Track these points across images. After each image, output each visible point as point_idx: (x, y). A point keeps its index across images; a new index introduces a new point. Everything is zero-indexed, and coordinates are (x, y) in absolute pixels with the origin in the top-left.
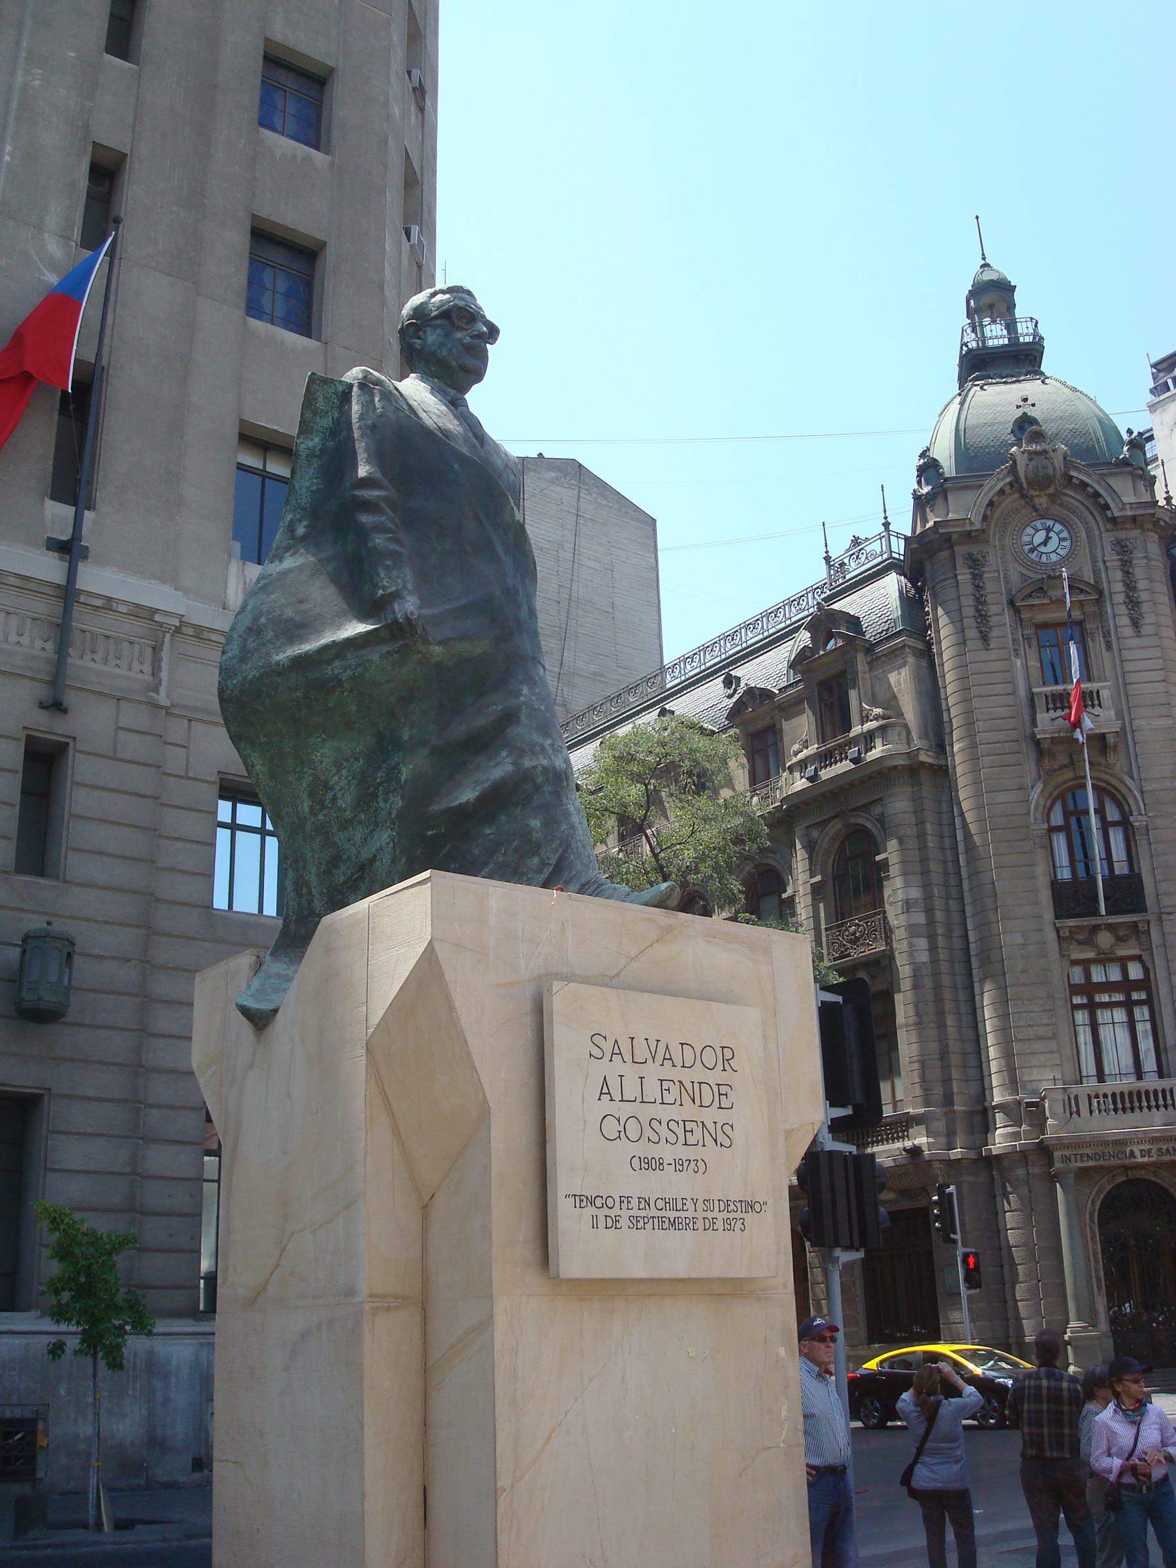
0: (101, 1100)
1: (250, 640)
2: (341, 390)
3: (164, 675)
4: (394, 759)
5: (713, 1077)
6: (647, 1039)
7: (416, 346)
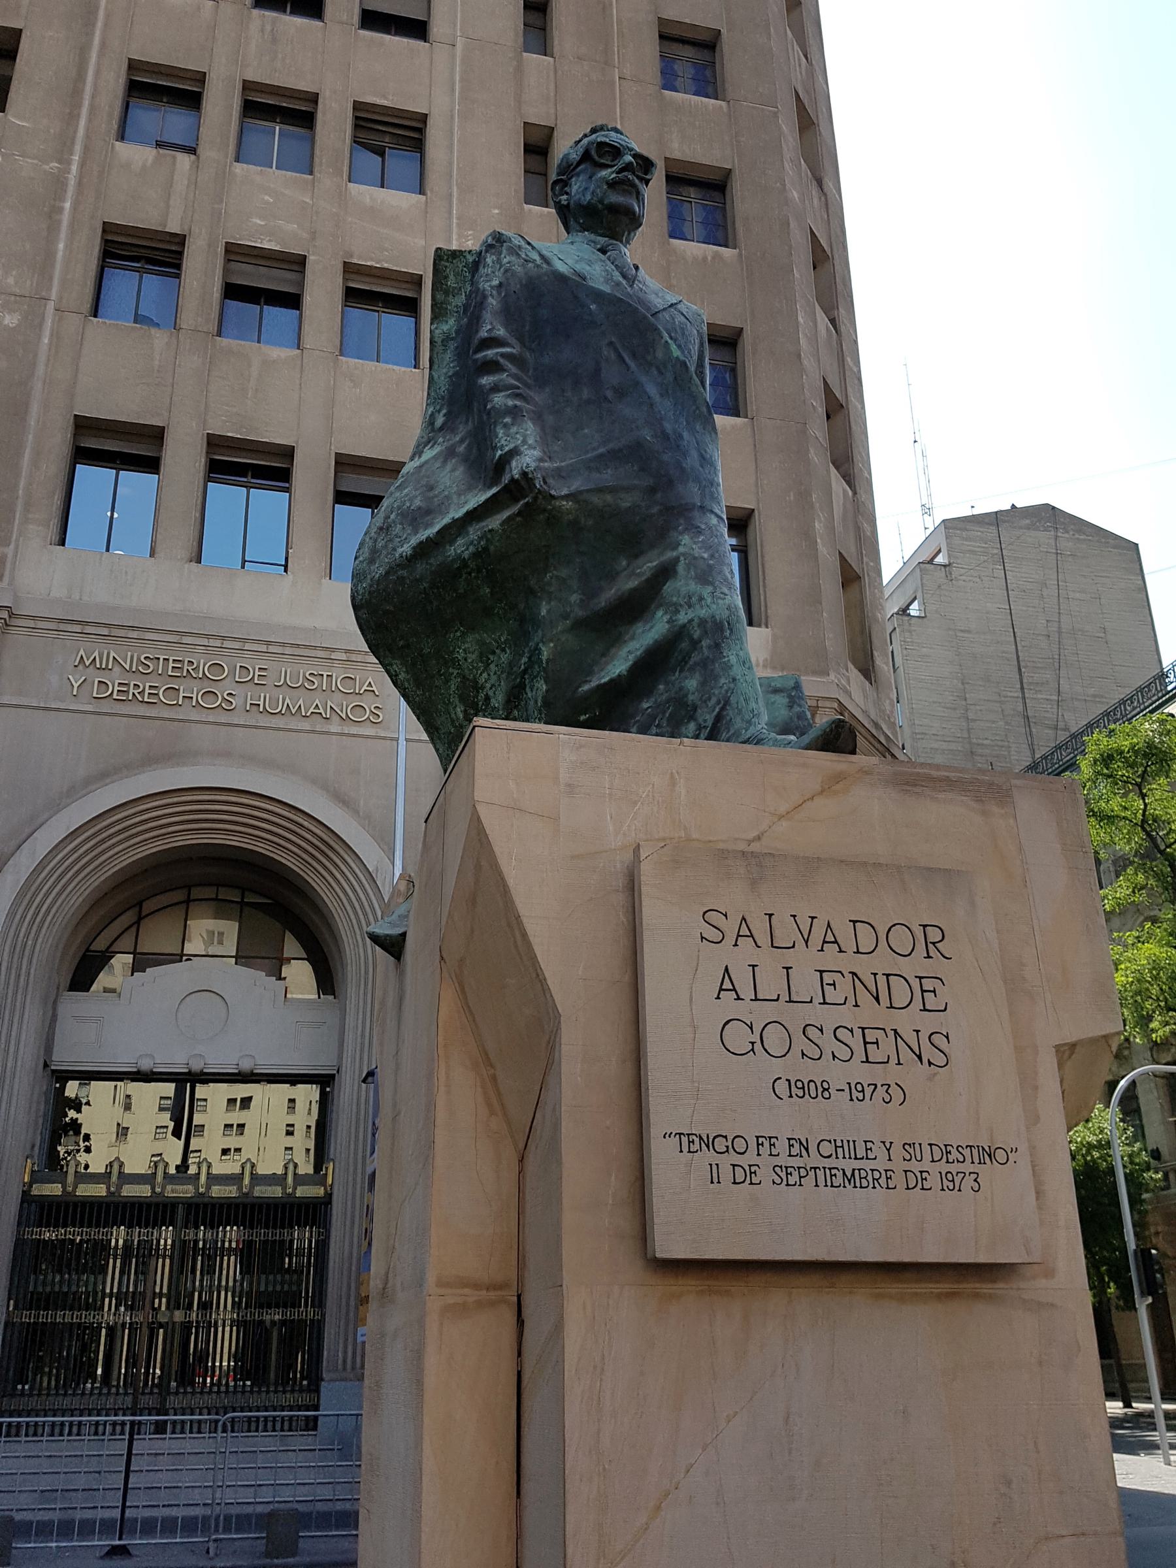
6: (794, 916)
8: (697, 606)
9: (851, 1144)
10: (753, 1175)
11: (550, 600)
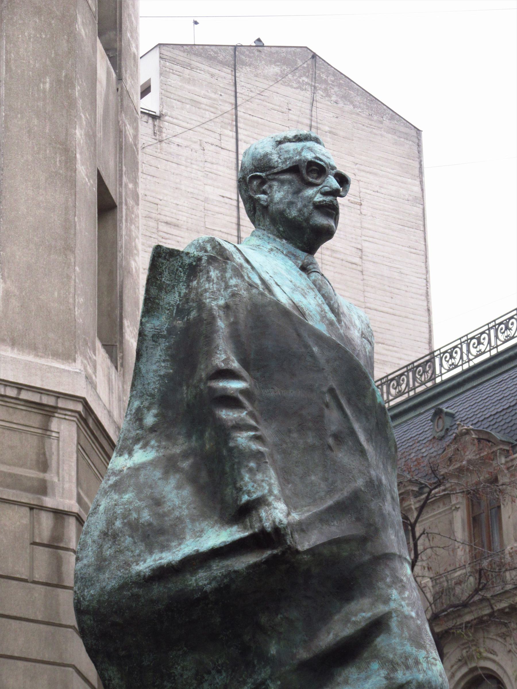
1: (105, 547)
2: (187, 262)
4: (260, 674)
7: (262, 202)
8: (415, 670)
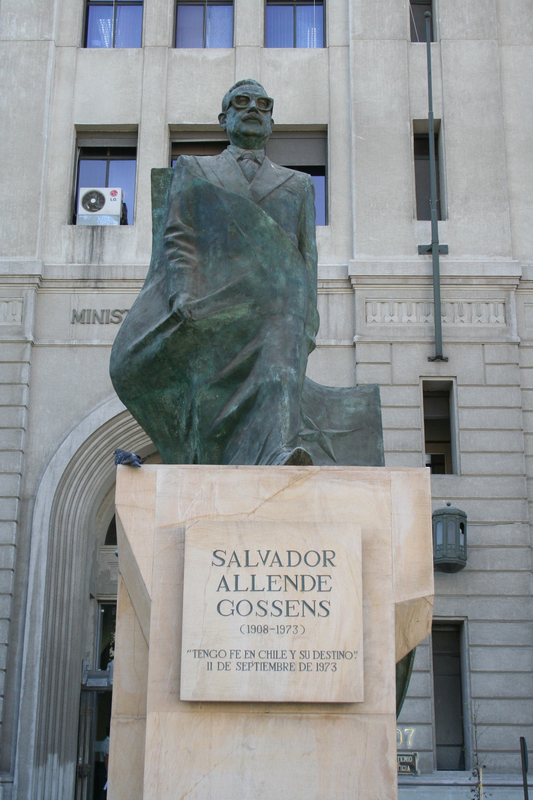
0: (504, 621)
3: (514, 320)
5: (314, 572)
6: (259, 551)
9: (275, 652)
10: (227, 667)
11: (199, 373)
